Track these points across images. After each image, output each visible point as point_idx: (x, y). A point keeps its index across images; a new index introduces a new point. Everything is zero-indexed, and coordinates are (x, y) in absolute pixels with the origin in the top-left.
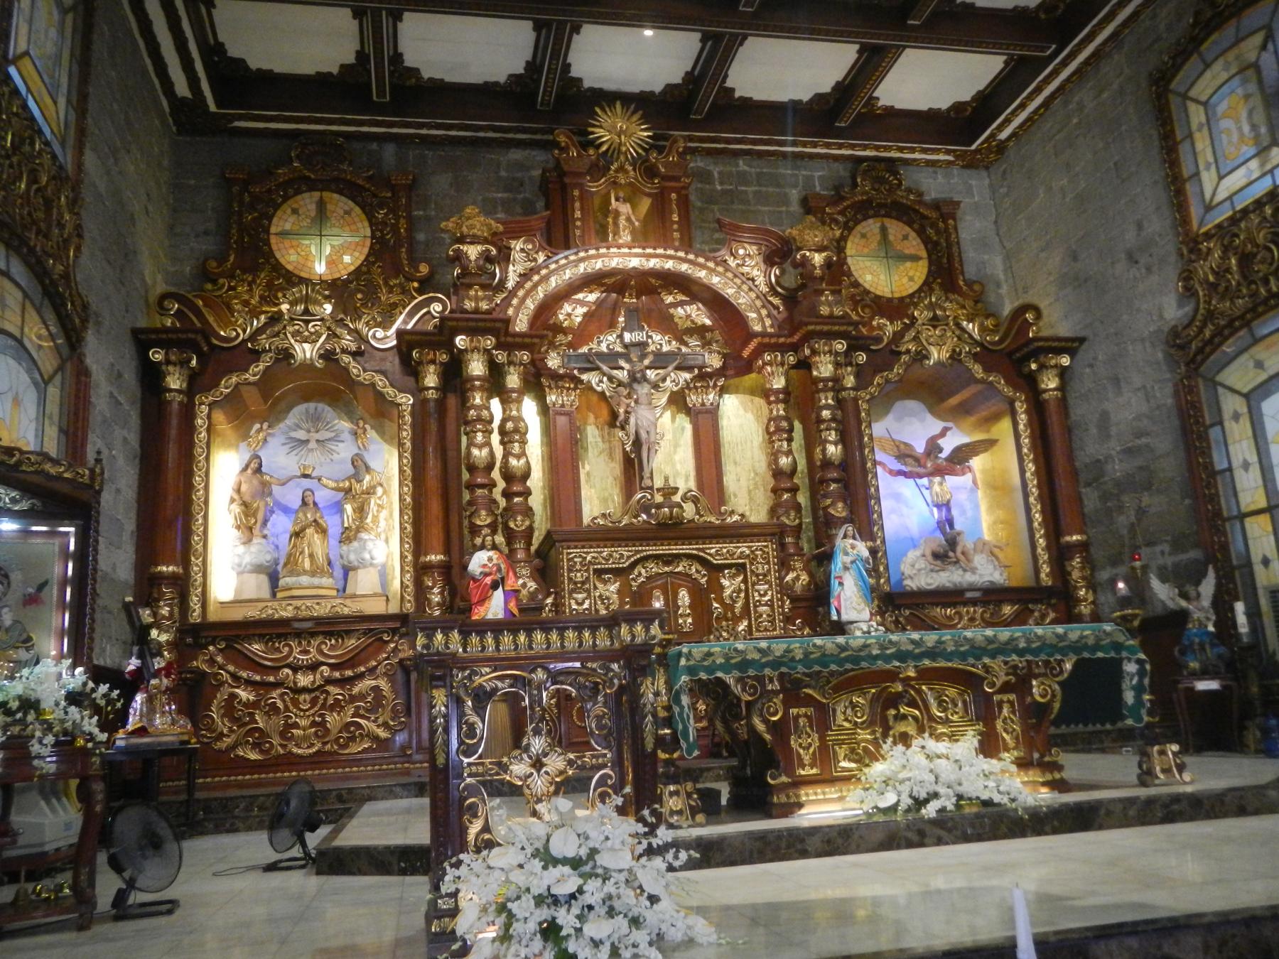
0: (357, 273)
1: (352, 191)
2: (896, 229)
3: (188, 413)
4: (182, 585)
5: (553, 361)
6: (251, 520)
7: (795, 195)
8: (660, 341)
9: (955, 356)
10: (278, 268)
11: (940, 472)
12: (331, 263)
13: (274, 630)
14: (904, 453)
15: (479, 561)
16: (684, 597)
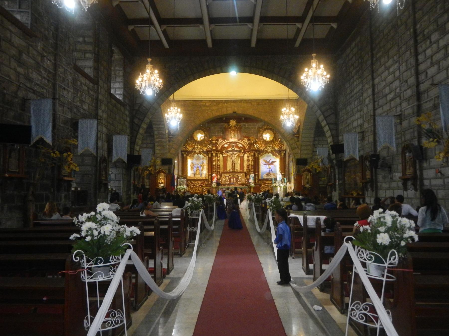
0: (203, 140)
1: (202, 130)
2: (269, 131)
3: (186, 158)
4: (186, 175)
5: (224, 152)
6: (192, 168)
7: (257, 127)
8: (236, 149)
9: (271, 151)
10: (194, 140)
11: (269, 164)
12: (200, 139)
13: (195, 180)
14: (266, 162)
15: (214, 175)
16: (235, 179)
